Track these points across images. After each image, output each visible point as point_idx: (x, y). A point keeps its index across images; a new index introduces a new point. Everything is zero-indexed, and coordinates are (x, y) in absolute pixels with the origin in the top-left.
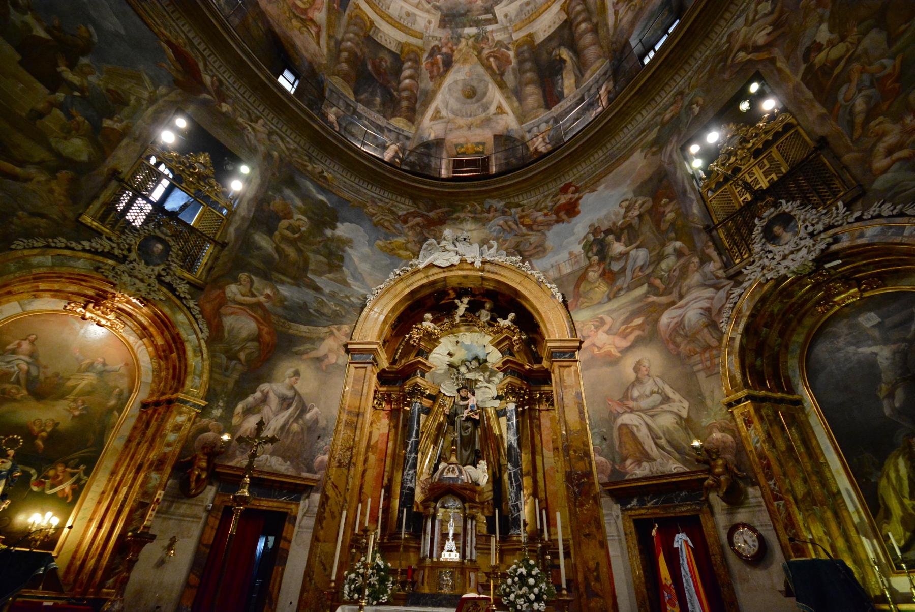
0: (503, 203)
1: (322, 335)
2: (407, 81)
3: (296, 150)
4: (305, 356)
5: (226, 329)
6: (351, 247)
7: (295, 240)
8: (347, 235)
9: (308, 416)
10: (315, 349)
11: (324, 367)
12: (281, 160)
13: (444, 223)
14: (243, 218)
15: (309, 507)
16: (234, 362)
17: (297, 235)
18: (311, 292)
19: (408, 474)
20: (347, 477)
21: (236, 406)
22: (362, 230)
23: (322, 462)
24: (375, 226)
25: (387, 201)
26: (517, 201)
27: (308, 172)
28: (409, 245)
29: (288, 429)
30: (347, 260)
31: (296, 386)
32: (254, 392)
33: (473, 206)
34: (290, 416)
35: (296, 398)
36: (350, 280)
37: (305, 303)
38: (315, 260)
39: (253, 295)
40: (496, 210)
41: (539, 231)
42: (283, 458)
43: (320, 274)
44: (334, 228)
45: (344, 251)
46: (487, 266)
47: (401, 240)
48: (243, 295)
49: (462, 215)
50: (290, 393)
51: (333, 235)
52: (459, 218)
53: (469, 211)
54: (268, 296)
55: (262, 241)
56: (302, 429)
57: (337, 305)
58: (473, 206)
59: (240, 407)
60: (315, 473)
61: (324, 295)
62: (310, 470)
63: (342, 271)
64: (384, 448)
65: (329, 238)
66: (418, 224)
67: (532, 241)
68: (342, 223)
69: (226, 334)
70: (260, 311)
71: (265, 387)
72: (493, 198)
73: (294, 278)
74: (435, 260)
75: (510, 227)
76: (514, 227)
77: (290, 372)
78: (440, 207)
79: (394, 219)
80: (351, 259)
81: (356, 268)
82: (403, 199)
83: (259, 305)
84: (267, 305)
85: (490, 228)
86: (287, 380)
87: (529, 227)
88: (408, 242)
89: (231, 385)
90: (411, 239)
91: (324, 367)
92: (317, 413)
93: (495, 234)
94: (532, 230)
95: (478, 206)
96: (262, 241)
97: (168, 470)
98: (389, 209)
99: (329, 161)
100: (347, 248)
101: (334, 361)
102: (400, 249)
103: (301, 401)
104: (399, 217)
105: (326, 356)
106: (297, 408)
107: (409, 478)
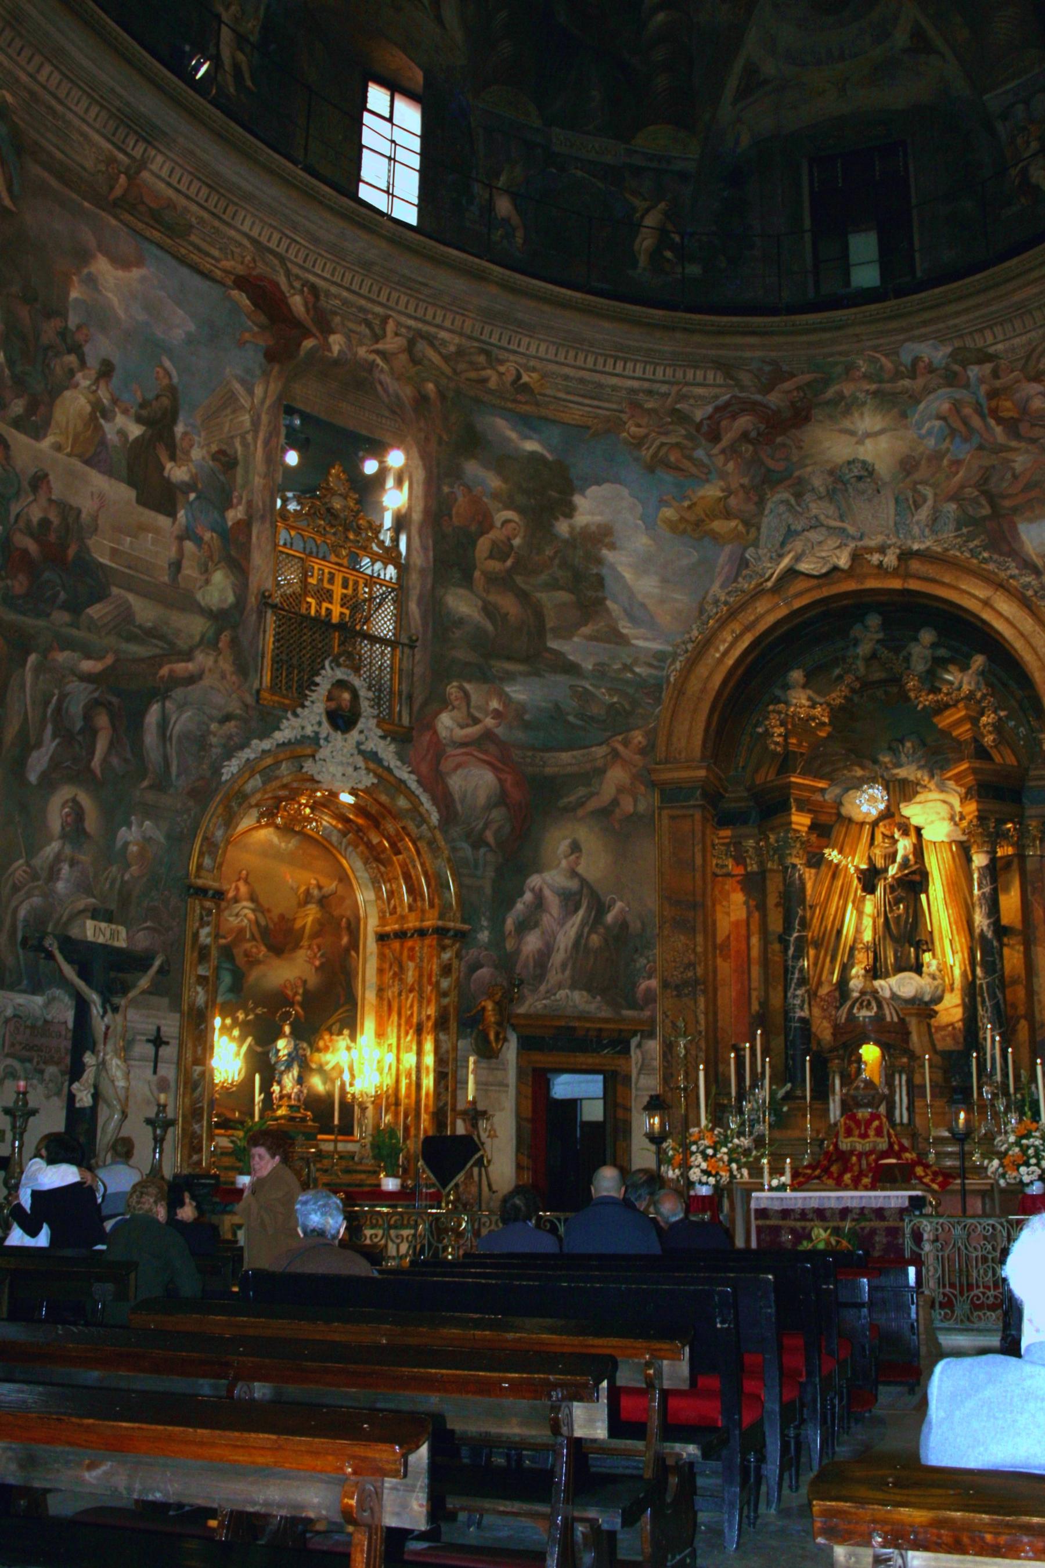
0: (949, 349)
1: (599, 763)
2: (661, 17)
3: (460, 353)
4: (580, 812)
5: (456, 797)
6: (612, 547)
7: (510, 571)
8: (598, 518)
9: (610, 918)
10: (592, 795)
11: (617, 826)
12: (442, 395)
13: (807, 419)
14: (422, 572)
15: (643, 1059)
16: (482, 850)
17: (509, 563)
18: (561, 678)
19: (795, 996)
20: (695, 1012)
21: (504, 921)
22: (625, 492)
23: (648, 990)
24: (651, 469)
25: (664, 388)
26: (980, 344)
27: (491, 392)
28: (732, 501)
29: (586, 944)
30: (609, 581)
31: (580, 869)
32: (521, 894)
33: (873, 360)
34: (583, 924)
35: (585, 891)
36: (625, 628)
37: (557, 705)
38: (553, 601)
39: (476, 721)
40: (931, 369)
41: (1033, 441)
42: (589, 991)
43: (566, 632)
44: (569, 510)
45: (599, 561)
46: (915, 565)
47: (712, 491)
48: (462, 727)
49: (848, 389)
50: (573, 885)
51: (572, 528)
52: (841, 396)
53: (867, 377)
54: (497, 714)
55: (462, 604)
56: (606, 940)
57: (611, 691)
58: (873, 360)
59: (509, 924)
60: (642, 1009)
61: (584, 678)
62: (633, 1005)
63: (607, 611)
64: (744, 947)
65: (566, 542)
66: (745, 436)
67: (1018, 467)
68: (582, 492)
69: (459, 807)
70: (492, 748)
71: (535, 881)
72: (923, 338)
73: (526, 660)
74: (798, 559)
75: (965, 422)
76: (976, 422)
77: (564, 846)
78: (793, 375)
79: (689, 437)
80: (620, 578)
81: (632, 596)
82: (700, 373)
83: (488, 735)
84: (499, 731)
85: (919, 425)
86: (564, 863)
87: (1012, 426)
88: (729, 492)
89: (488, 890)
90: (734, 485)
91: (617, 826)
92: (622, 911)
93: (931, 442)
94: (1017, 436)
95: (883, 359)
96: (462, 604)
97: (453, 1025)
98: (674, 412)
99: (525, 340)
100: (605, 552)
101: (631, 809)
102: (712, 516)
103: (593, 893)
104: (698, 427)
105: (615, 802)
106: (589, 909)
107: (798, 1002)
